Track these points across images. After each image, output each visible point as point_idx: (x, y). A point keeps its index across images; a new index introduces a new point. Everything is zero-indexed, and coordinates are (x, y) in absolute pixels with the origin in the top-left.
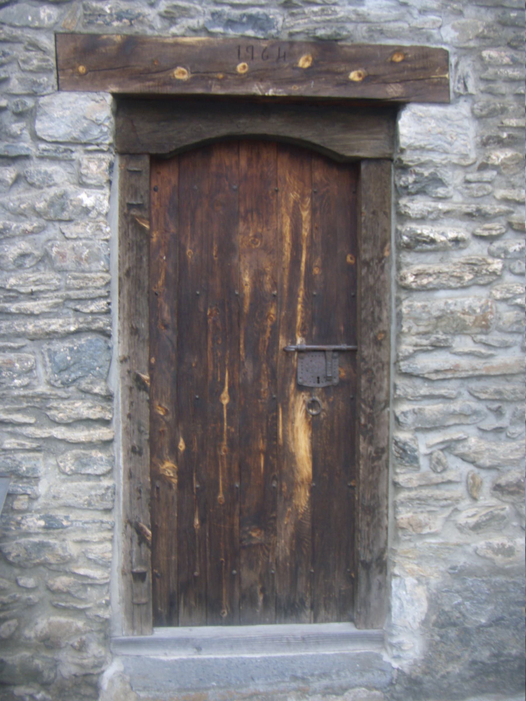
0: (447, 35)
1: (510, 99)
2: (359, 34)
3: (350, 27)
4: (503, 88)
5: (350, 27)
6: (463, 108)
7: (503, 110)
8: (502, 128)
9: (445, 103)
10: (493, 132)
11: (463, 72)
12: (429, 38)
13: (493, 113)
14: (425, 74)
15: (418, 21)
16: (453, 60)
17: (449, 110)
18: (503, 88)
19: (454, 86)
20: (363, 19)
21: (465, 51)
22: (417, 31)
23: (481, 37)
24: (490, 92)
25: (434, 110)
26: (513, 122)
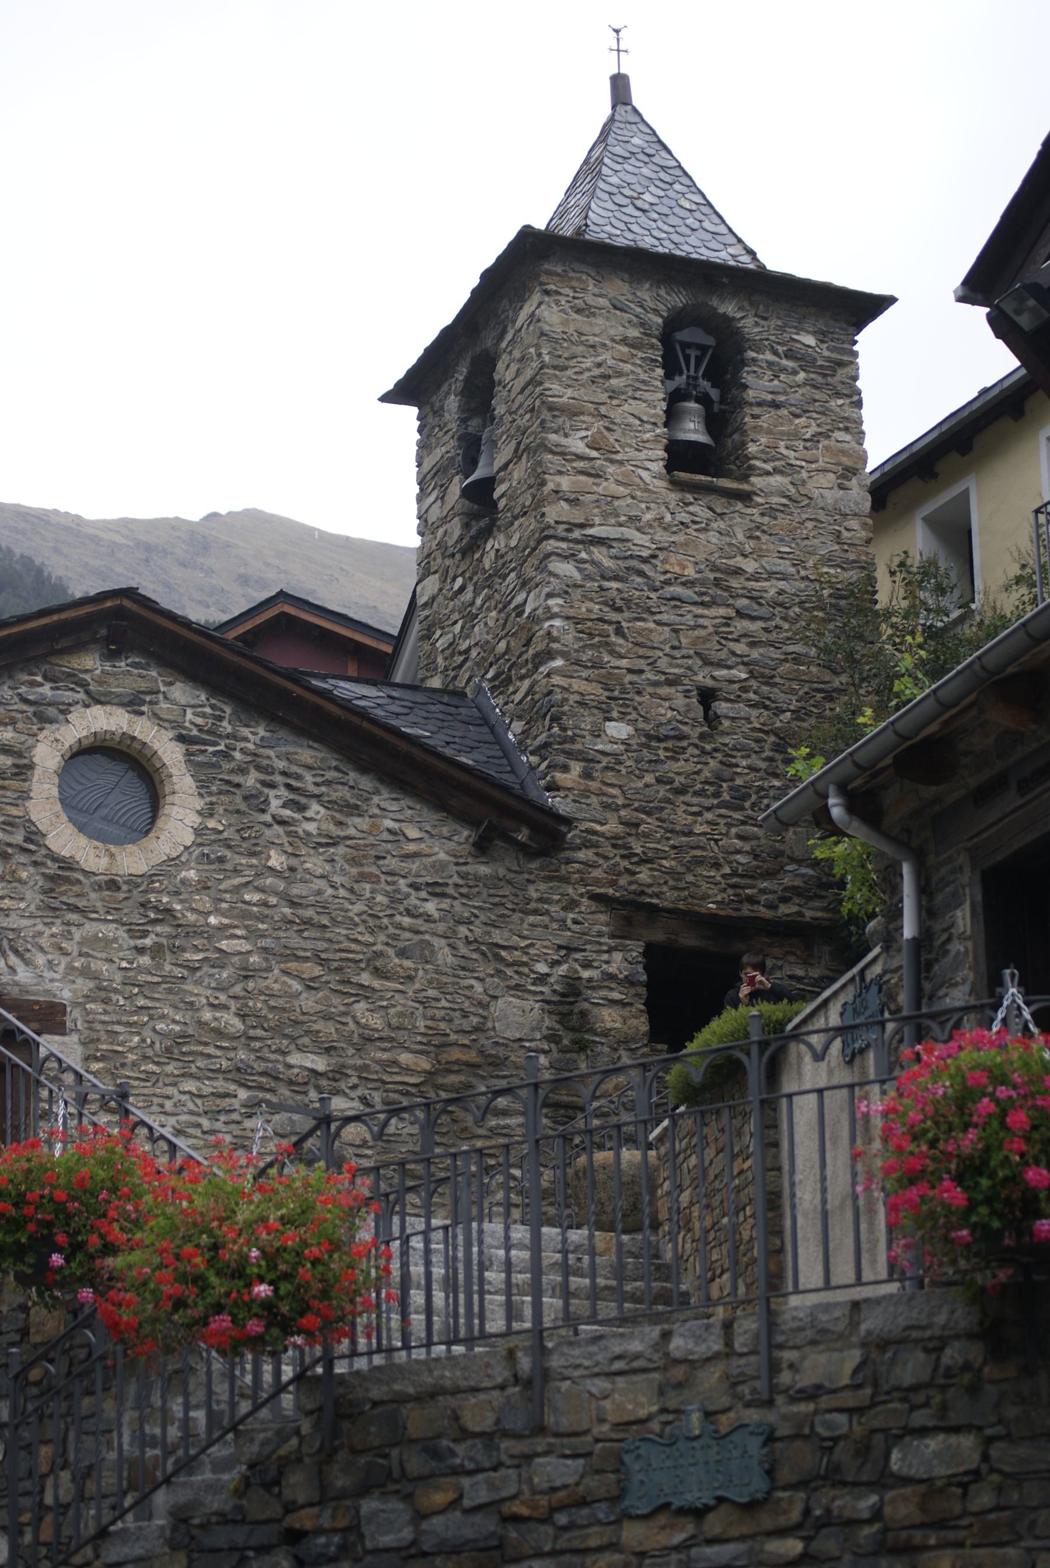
0: (66, 995)
1: (102, 1033)
2: (15, 992)
3: (9, 988)
4: (98, 1027)
5: (9, 988)
6: (75, 1038)
7: (98, 1040)
8: (97, 1050)
9: (64, 1034)
10: (92, 1052)
11: (74, 1017)
12: (55, 996)
13: (92, 1041)
14: (51, 1017)
15: (49, 986)
16: (69, 1009)
17: (66, 1039)
18: (98, 1027)
19: (69, 1024)
20: (16, 984)
21: (76, 1004)
22: (48, 992)
23: (86, 996)
24: (91, 1029)
25: (57, 1038)
26: (104, 1047)
